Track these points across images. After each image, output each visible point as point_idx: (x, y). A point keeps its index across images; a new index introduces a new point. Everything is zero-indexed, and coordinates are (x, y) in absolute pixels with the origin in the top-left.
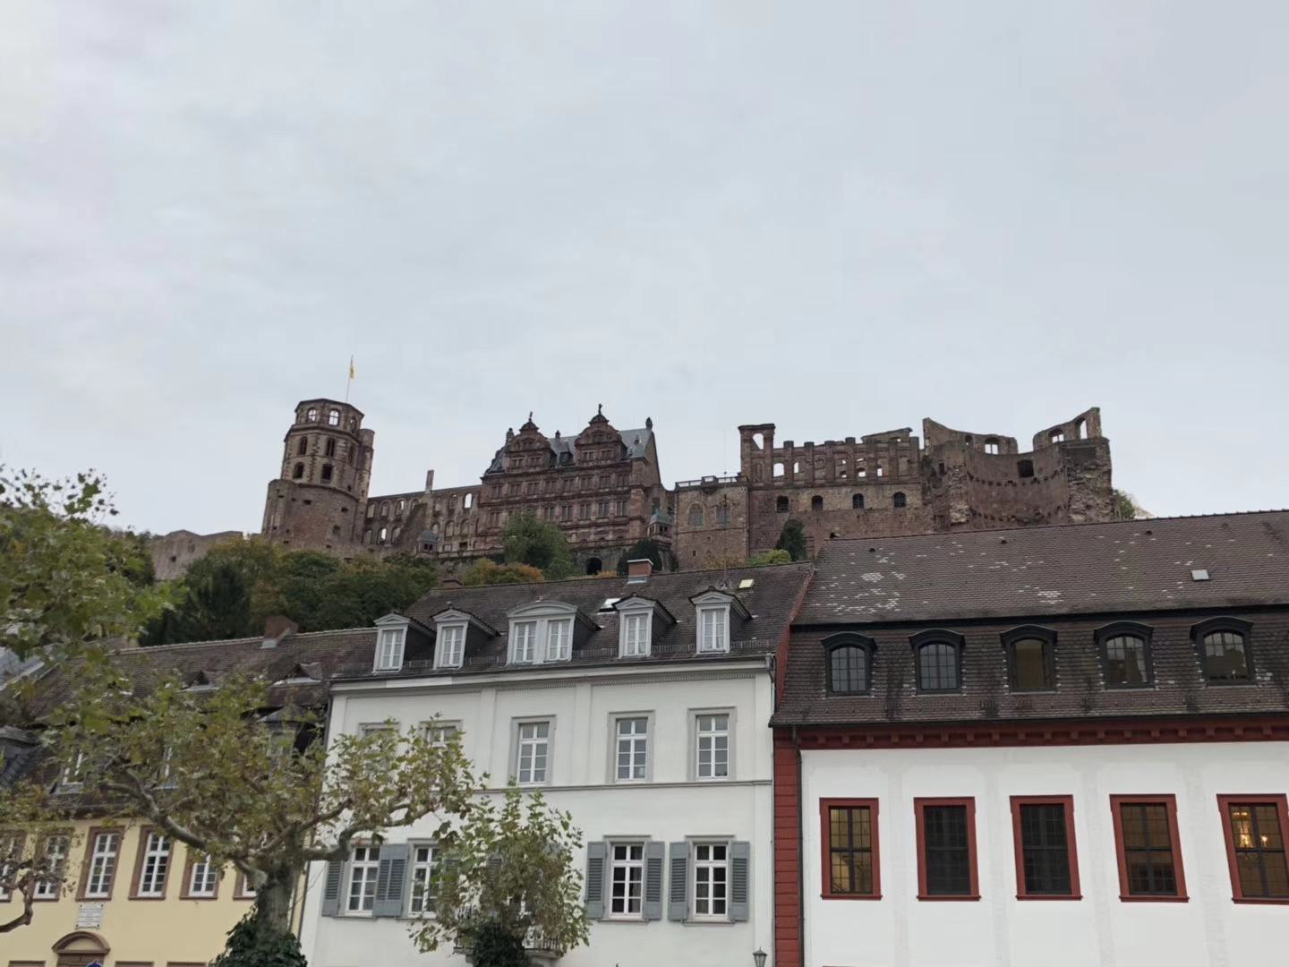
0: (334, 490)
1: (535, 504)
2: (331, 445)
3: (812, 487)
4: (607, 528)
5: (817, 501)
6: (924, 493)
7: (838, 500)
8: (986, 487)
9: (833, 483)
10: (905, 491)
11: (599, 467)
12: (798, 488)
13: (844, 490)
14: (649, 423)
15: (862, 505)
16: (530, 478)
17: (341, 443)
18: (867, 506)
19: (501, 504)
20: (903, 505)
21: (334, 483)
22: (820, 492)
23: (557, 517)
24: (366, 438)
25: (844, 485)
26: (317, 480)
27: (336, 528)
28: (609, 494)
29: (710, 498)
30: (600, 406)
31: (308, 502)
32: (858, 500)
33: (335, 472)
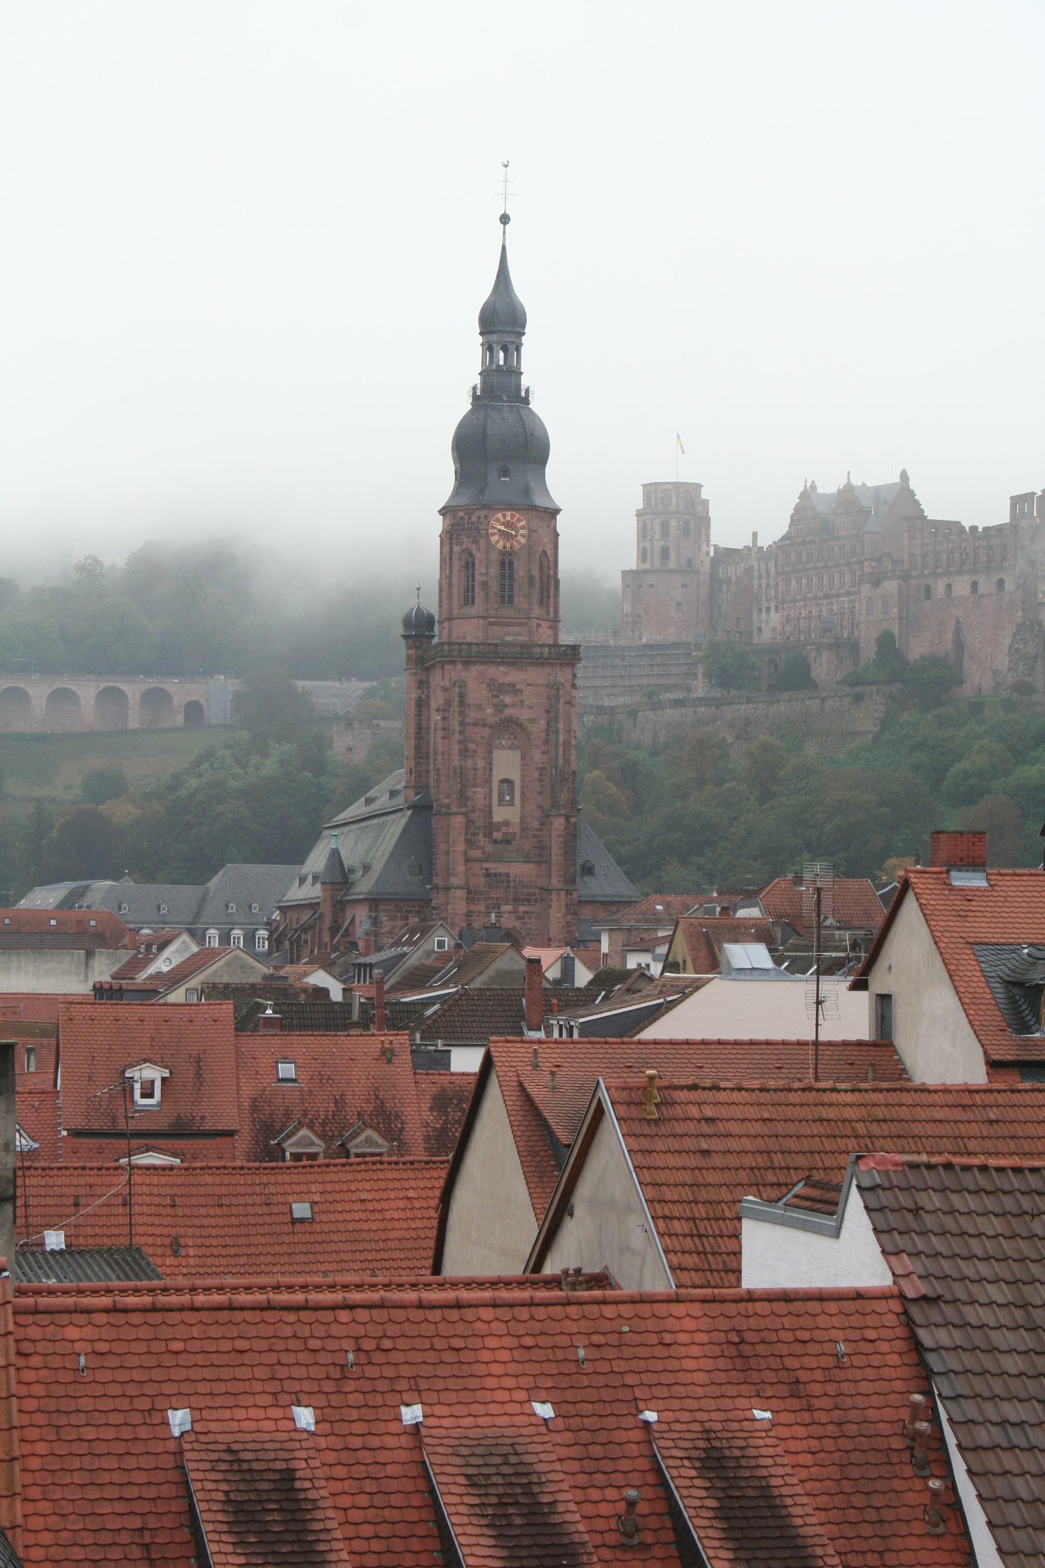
0: (672, 571)
2: (665, 526)
5: (949, 587)
7: (962, 586)
13: (966, 578)
14: (904, 476)
17: (673, 523)
18: (980, 593)
21: (672, 564)
24: (699, 509)
26: (657, 563)
27: (679, 604)
30: (849, 473)
31: (652, 586)
32: (975, 585)
33: (672, 551)
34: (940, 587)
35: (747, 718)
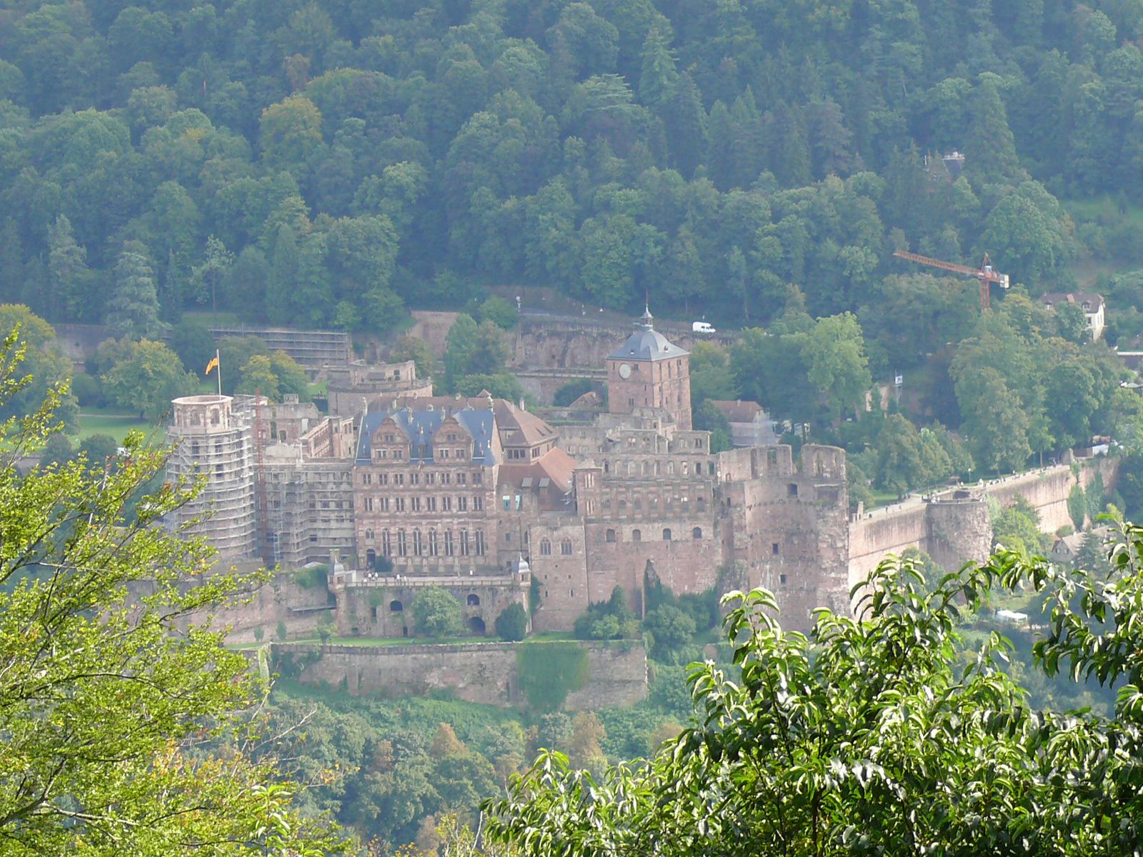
1: (403, 494)
3: (633, 522)
4: (467, 520)
5: (637, 533)
6: (716, 525)
8: (762, 508)
9: (650, 520)
10: (700, 526)
11: (455, 465)
12: (621, 521)
13: (656, 525)
15: (670, 538)
16: (395, 469)
18: (673, 538)
19: (371, 491)
20: (700, 536)
22: (639, 527)
23: (423, 507)
25: (655, 521)
28: (466, 489)
29: (555, 533)
32: (667, 533)
34: (627, 532)
35: (481, 665)
